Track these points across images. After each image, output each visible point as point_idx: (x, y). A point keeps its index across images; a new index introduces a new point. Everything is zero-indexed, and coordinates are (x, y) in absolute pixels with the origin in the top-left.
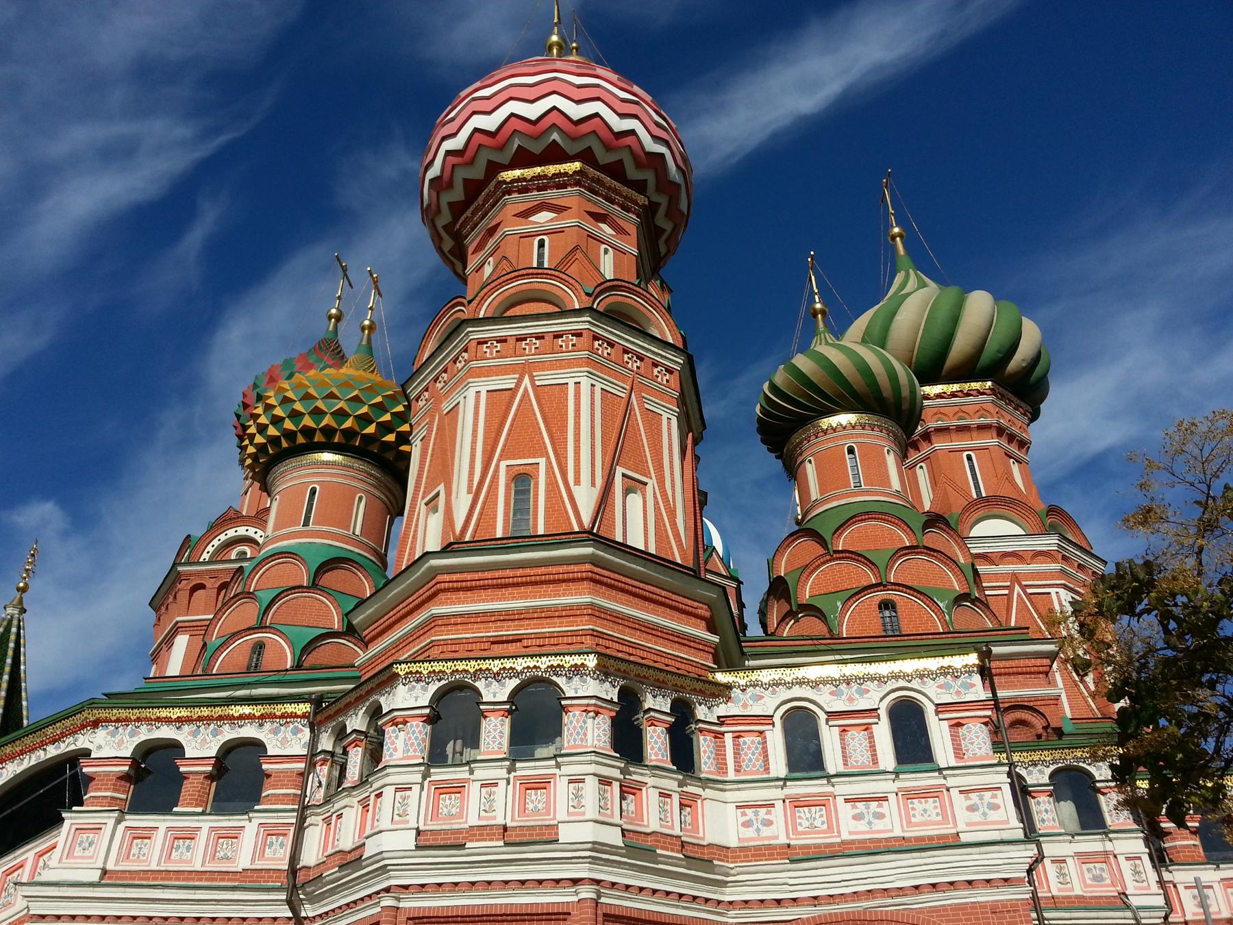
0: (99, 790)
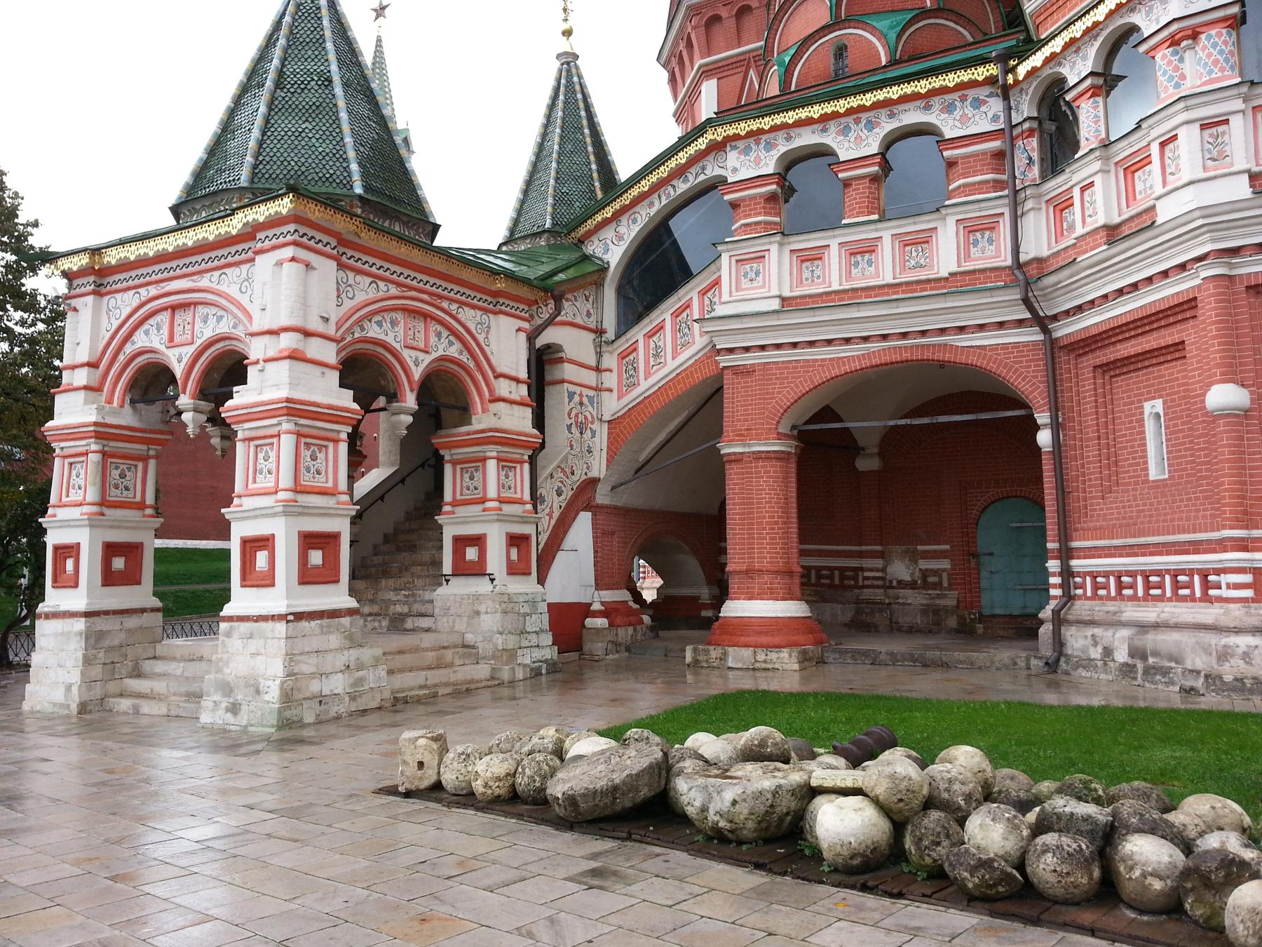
0: (749, 216)
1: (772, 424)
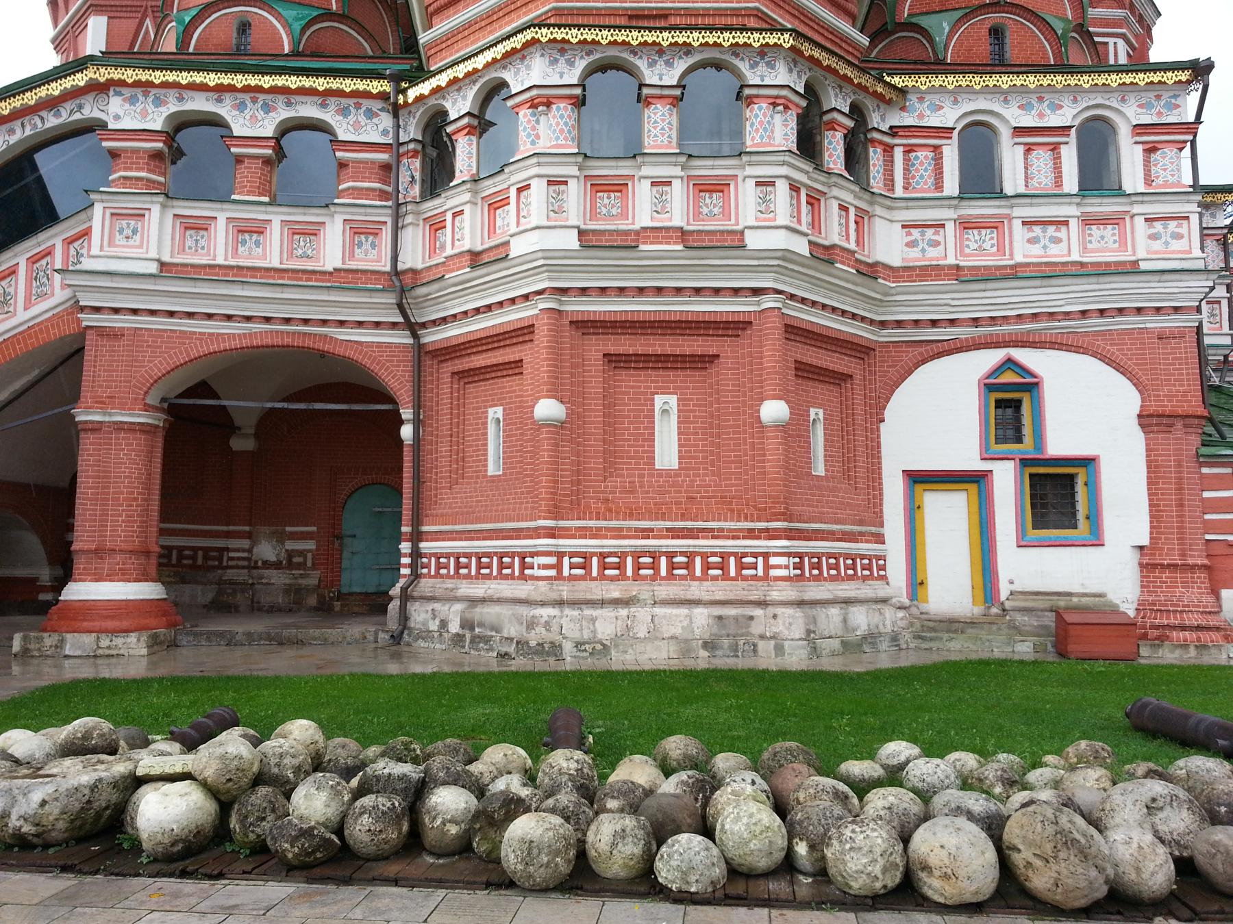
0: (130, 169)
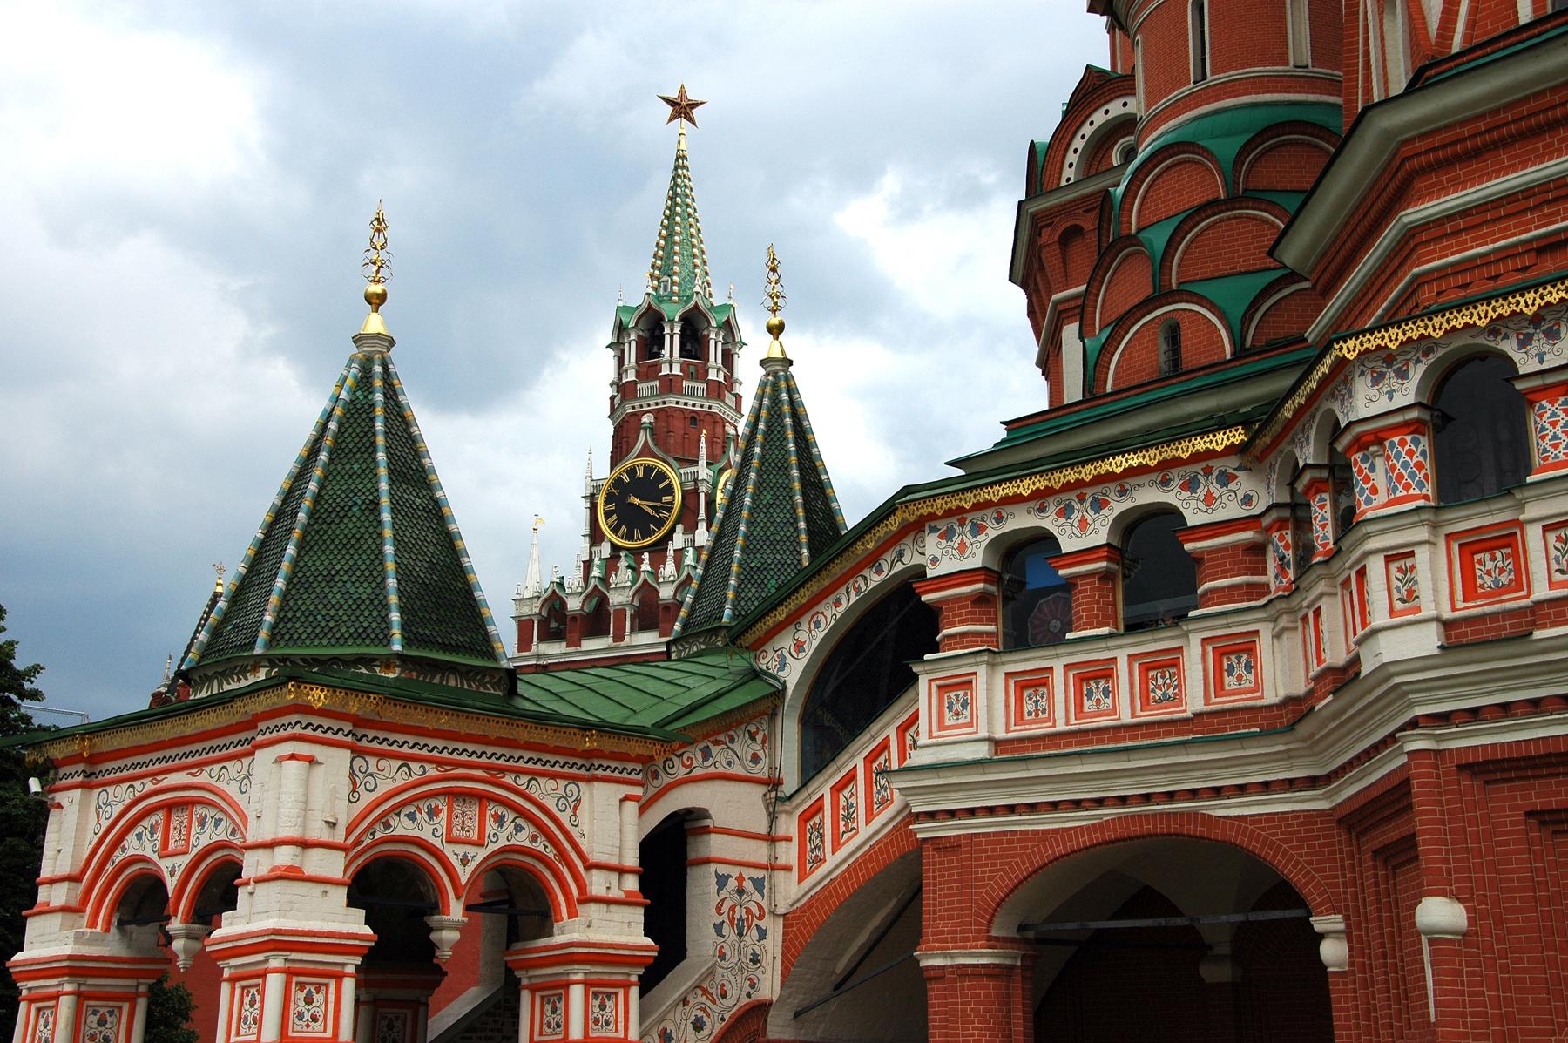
0: (953, 624)
1: (982, 924)
